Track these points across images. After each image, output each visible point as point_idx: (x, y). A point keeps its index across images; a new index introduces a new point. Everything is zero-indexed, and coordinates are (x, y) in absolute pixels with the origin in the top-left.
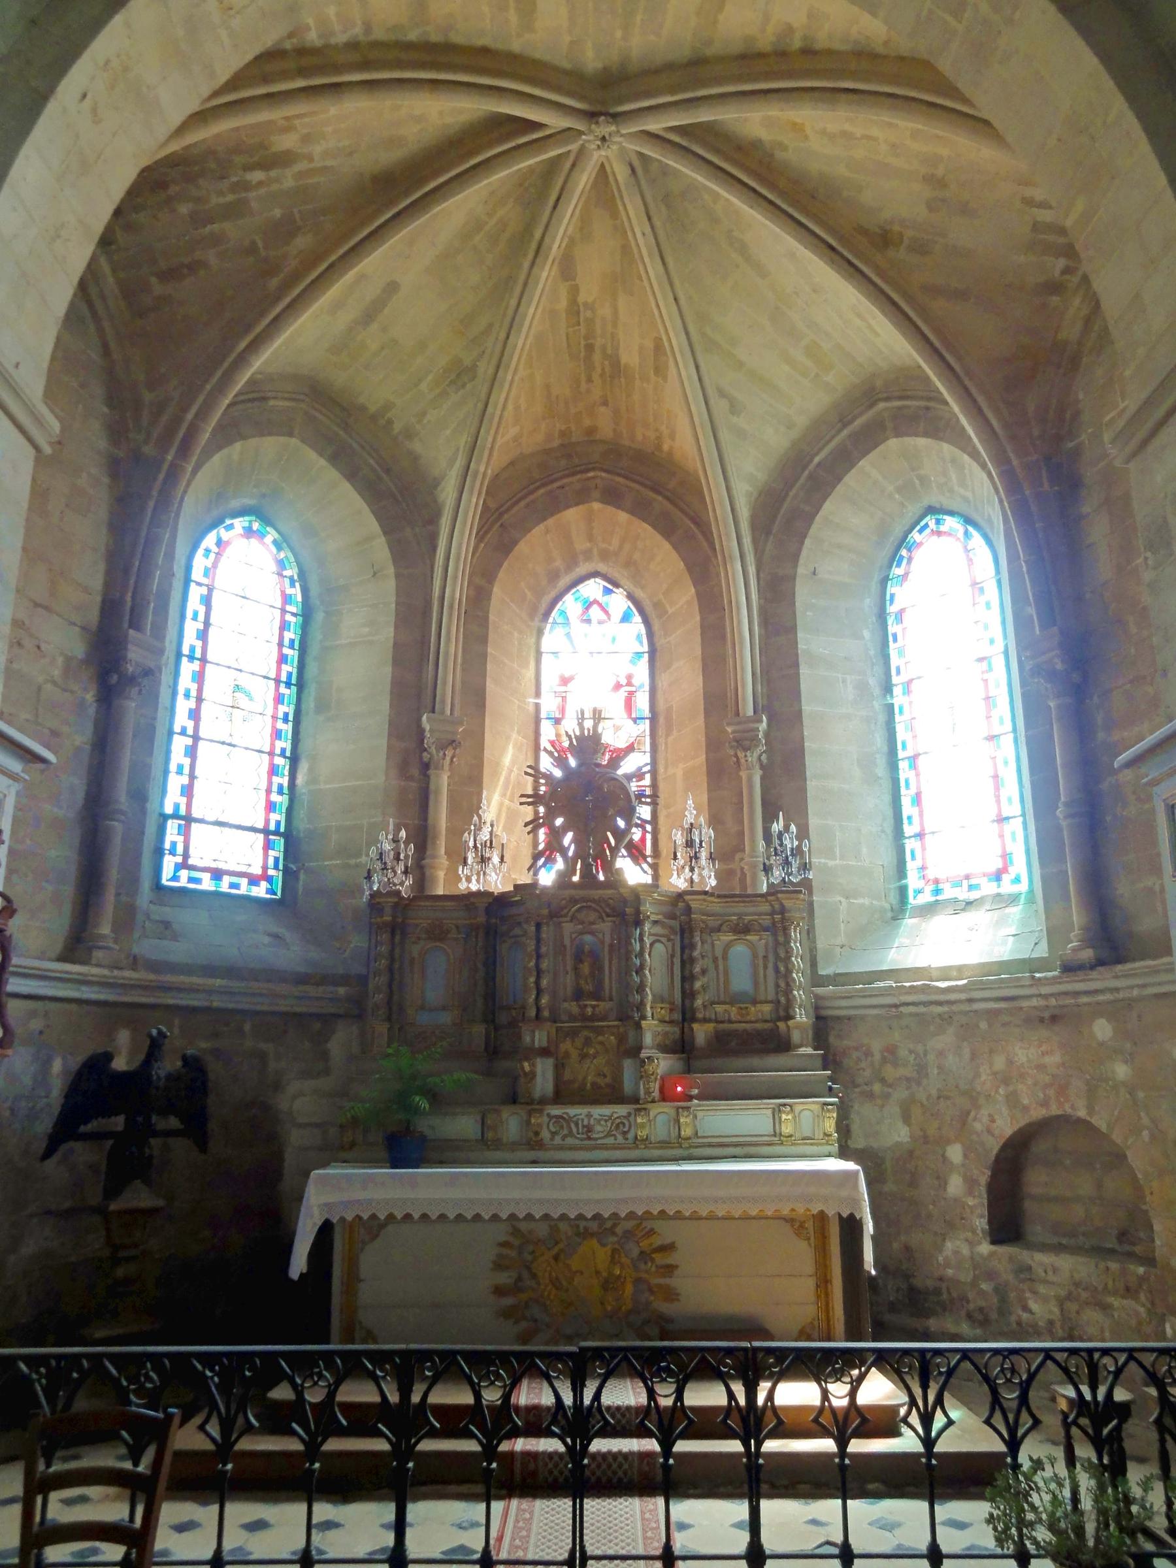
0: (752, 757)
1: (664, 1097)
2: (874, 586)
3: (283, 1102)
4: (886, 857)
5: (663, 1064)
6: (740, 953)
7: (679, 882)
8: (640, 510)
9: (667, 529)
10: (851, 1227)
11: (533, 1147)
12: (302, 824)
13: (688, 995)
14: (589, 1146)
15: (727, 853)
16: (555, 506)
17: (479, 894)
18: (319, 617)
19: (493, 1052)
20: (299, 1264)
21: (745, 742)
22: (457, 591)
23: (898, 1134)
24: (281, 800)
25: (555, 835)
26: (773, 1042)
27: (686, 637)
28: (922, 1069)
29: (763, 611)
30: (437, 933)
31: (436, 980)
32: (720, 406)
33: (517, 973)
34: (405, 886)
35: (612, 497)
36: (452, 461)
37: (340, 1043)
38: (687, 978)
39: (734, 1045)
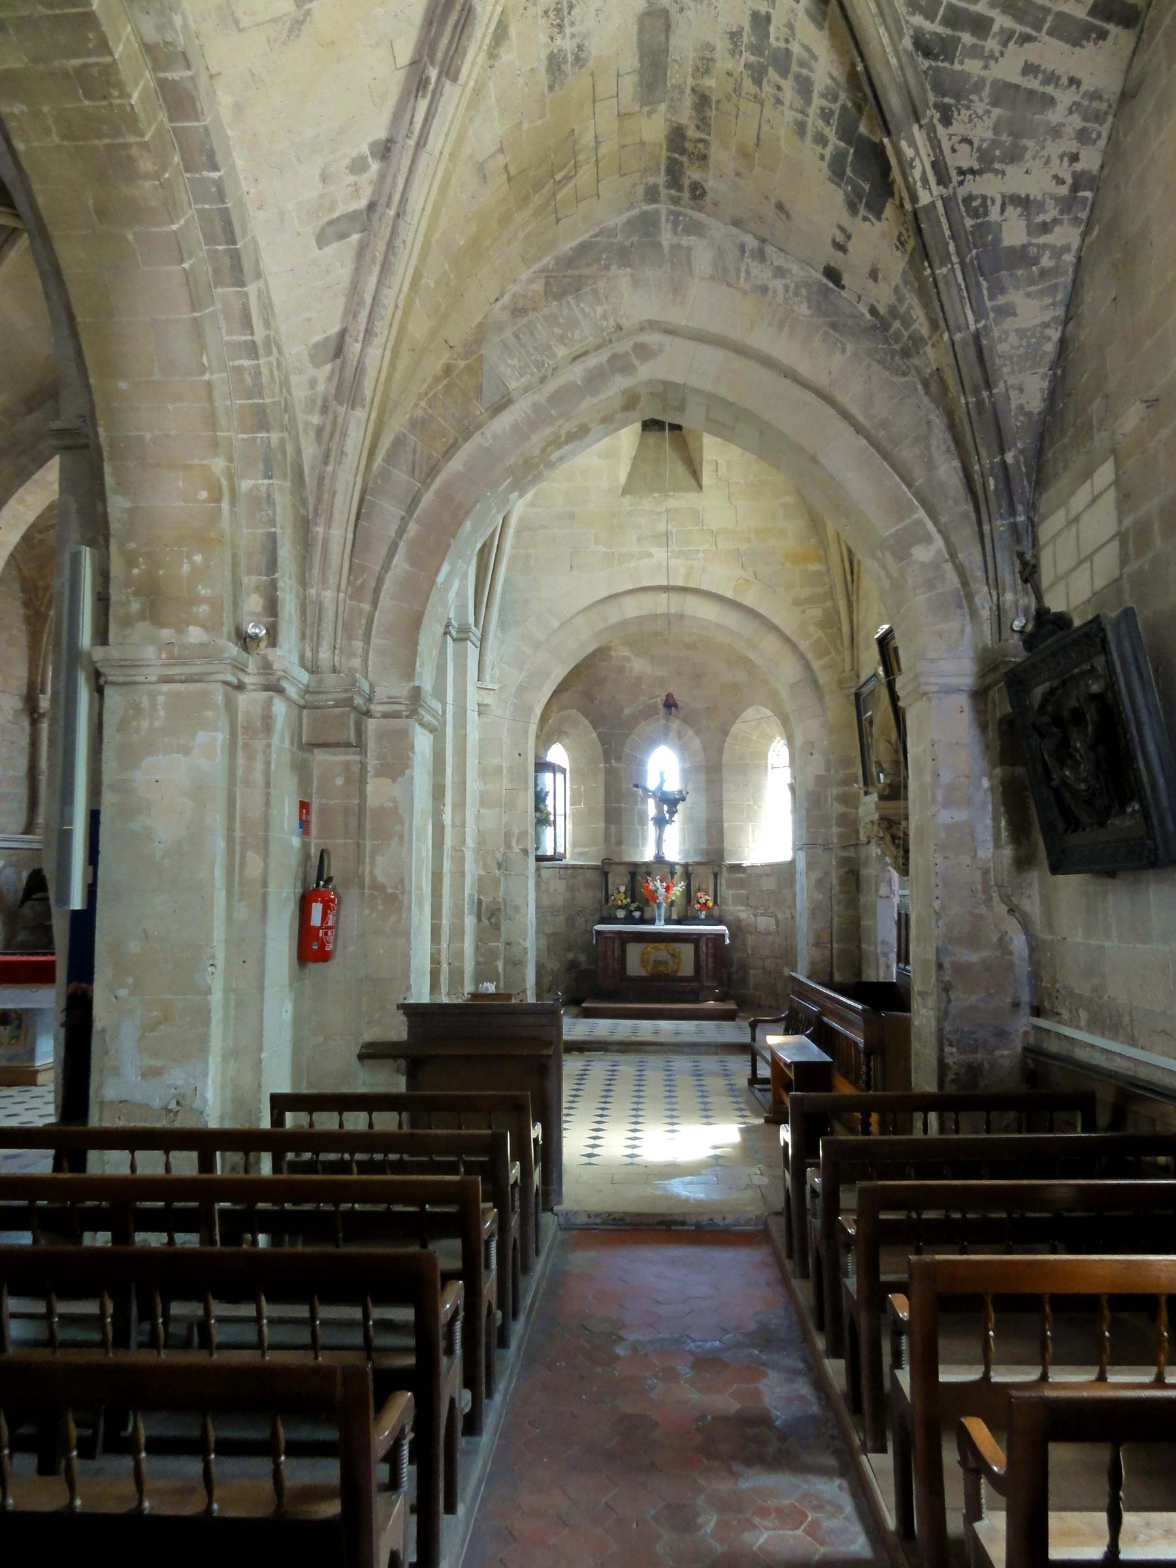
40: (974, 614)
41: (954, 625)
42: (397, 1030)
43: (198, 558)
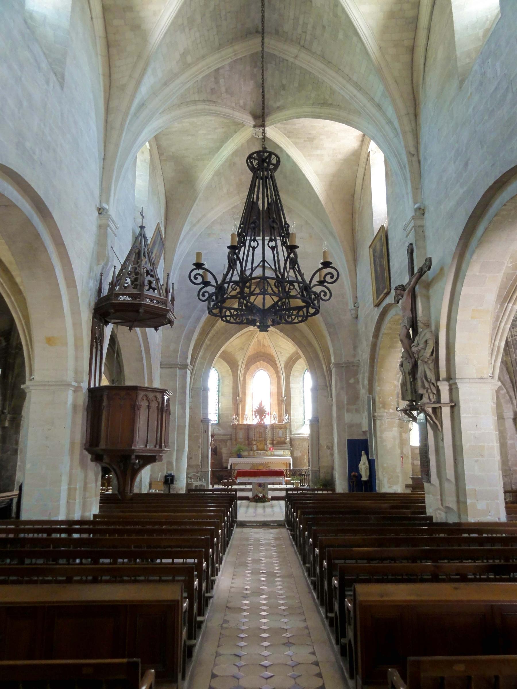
0: (284, 403)
1: (270, 450)
2: (302, 375)
3: (222, 451)
4: (303, 417)
5: (270, 446)
6: (280, 431)
7: (273, 422)
8: (268, 363)
9: (272, 366)
10: (290, 464)
11: (254, 456)
12: (220, 412)
13: (273, 437)
14: (261, 455)
15: (280, 416)
16: (256, 362)
17: (247, 424)
18: (221, 381)
19: (249, 444)
20: (229, 468)
21: (283, 401)
22: (241, 378)
23: (300, 454)
24: (217, 409)
25: (256, 416)
26: (284, 443)
27: (275, 381)
28: (302, 446)
29: (286, 380)
30: (241, 429)
31: (241, 435)
32: (279, 353)
33: (251, 434)
34: (237, 423)
35: (264, 360)
36: (240, 359)
37: (229, 443)
38: (273, 435)
39: (279, 443)
40: (512, 403)
41: (509, 405)
42: (410, 482)
43: (391, 398)
